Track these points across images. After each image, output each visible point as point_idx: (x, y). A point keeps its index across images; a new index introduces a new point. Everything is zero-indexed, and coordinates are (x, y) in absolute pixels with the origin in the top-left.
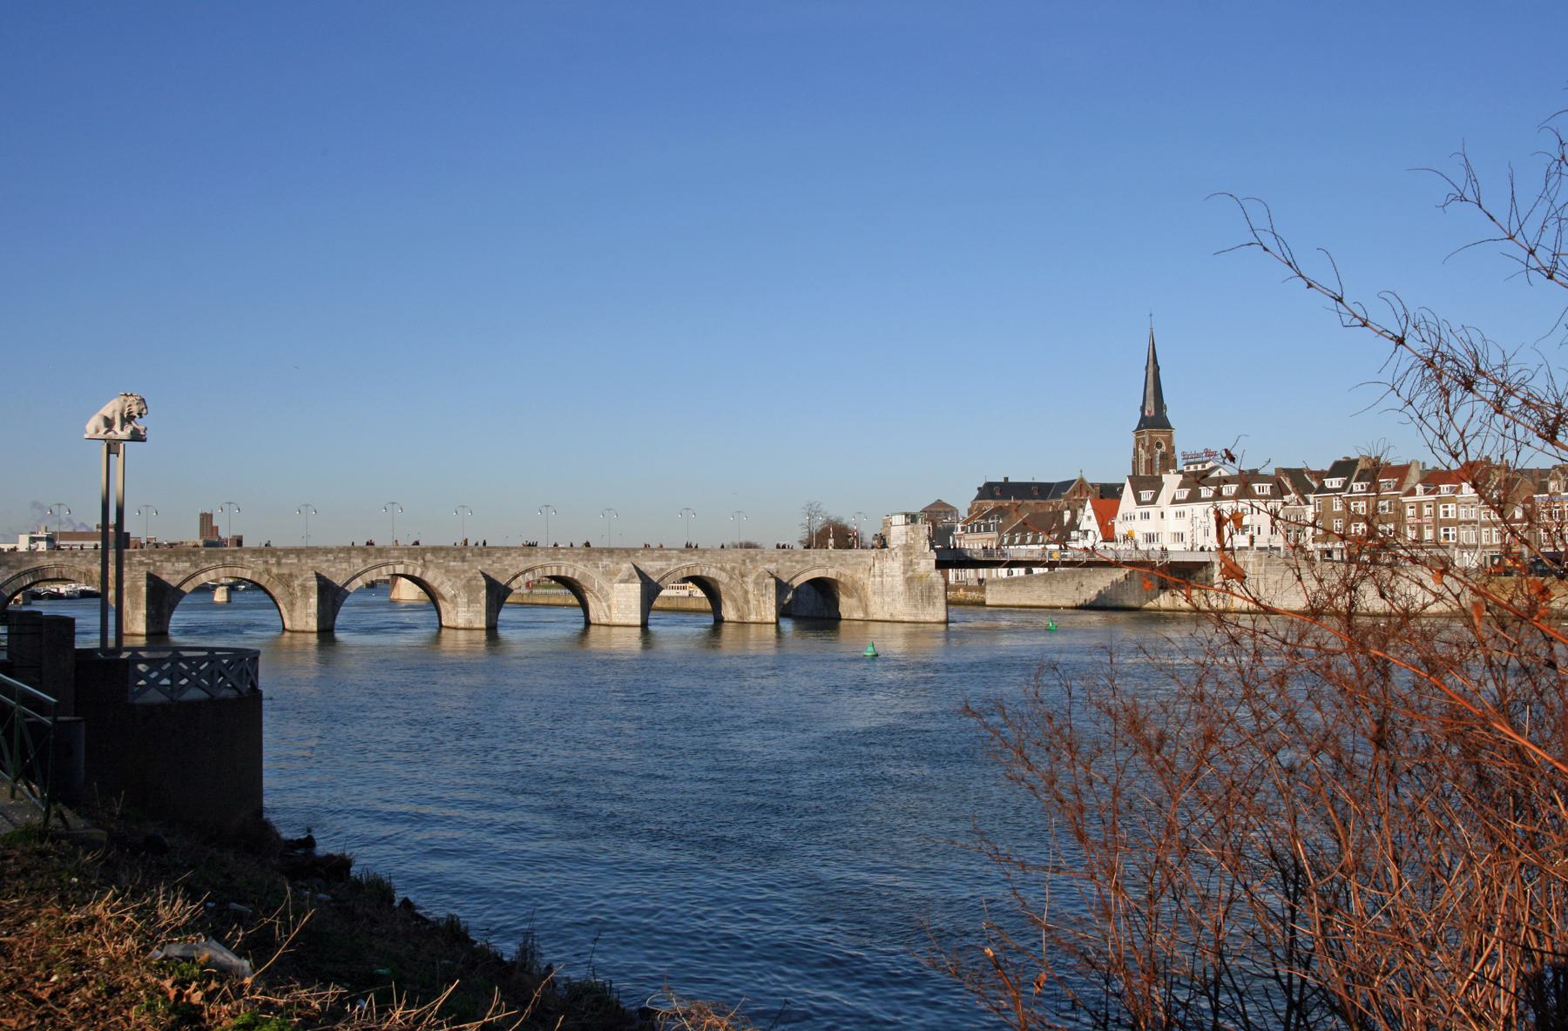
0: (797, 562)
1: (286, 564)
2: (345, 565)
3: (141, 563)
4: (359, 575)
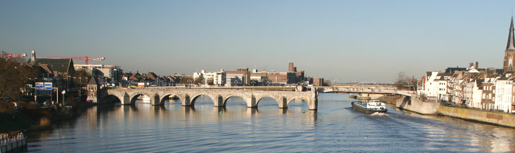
0: (291, 94)
1: (181, 92)
2: (192, 93)
3: (155, 92)
4: (195, 95)
